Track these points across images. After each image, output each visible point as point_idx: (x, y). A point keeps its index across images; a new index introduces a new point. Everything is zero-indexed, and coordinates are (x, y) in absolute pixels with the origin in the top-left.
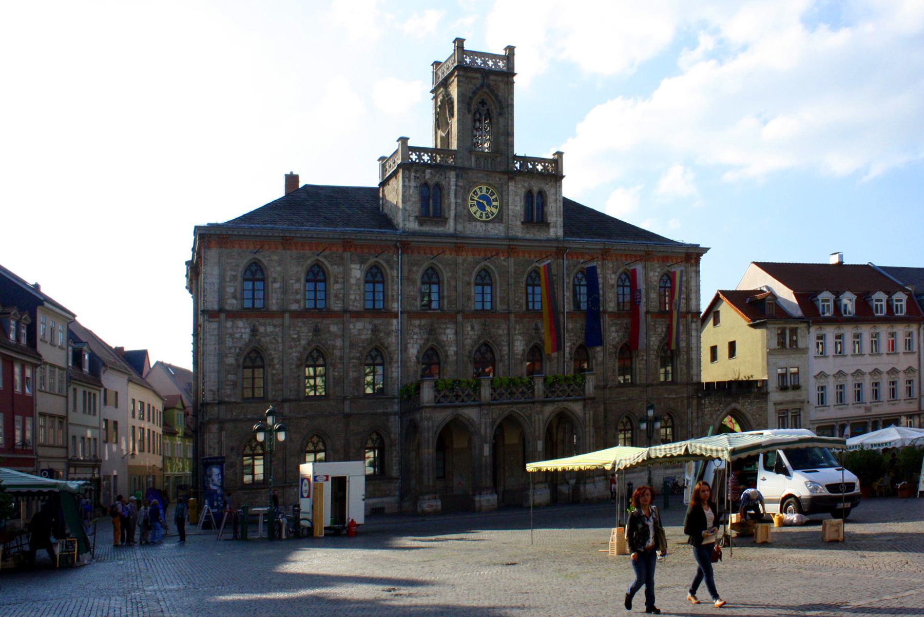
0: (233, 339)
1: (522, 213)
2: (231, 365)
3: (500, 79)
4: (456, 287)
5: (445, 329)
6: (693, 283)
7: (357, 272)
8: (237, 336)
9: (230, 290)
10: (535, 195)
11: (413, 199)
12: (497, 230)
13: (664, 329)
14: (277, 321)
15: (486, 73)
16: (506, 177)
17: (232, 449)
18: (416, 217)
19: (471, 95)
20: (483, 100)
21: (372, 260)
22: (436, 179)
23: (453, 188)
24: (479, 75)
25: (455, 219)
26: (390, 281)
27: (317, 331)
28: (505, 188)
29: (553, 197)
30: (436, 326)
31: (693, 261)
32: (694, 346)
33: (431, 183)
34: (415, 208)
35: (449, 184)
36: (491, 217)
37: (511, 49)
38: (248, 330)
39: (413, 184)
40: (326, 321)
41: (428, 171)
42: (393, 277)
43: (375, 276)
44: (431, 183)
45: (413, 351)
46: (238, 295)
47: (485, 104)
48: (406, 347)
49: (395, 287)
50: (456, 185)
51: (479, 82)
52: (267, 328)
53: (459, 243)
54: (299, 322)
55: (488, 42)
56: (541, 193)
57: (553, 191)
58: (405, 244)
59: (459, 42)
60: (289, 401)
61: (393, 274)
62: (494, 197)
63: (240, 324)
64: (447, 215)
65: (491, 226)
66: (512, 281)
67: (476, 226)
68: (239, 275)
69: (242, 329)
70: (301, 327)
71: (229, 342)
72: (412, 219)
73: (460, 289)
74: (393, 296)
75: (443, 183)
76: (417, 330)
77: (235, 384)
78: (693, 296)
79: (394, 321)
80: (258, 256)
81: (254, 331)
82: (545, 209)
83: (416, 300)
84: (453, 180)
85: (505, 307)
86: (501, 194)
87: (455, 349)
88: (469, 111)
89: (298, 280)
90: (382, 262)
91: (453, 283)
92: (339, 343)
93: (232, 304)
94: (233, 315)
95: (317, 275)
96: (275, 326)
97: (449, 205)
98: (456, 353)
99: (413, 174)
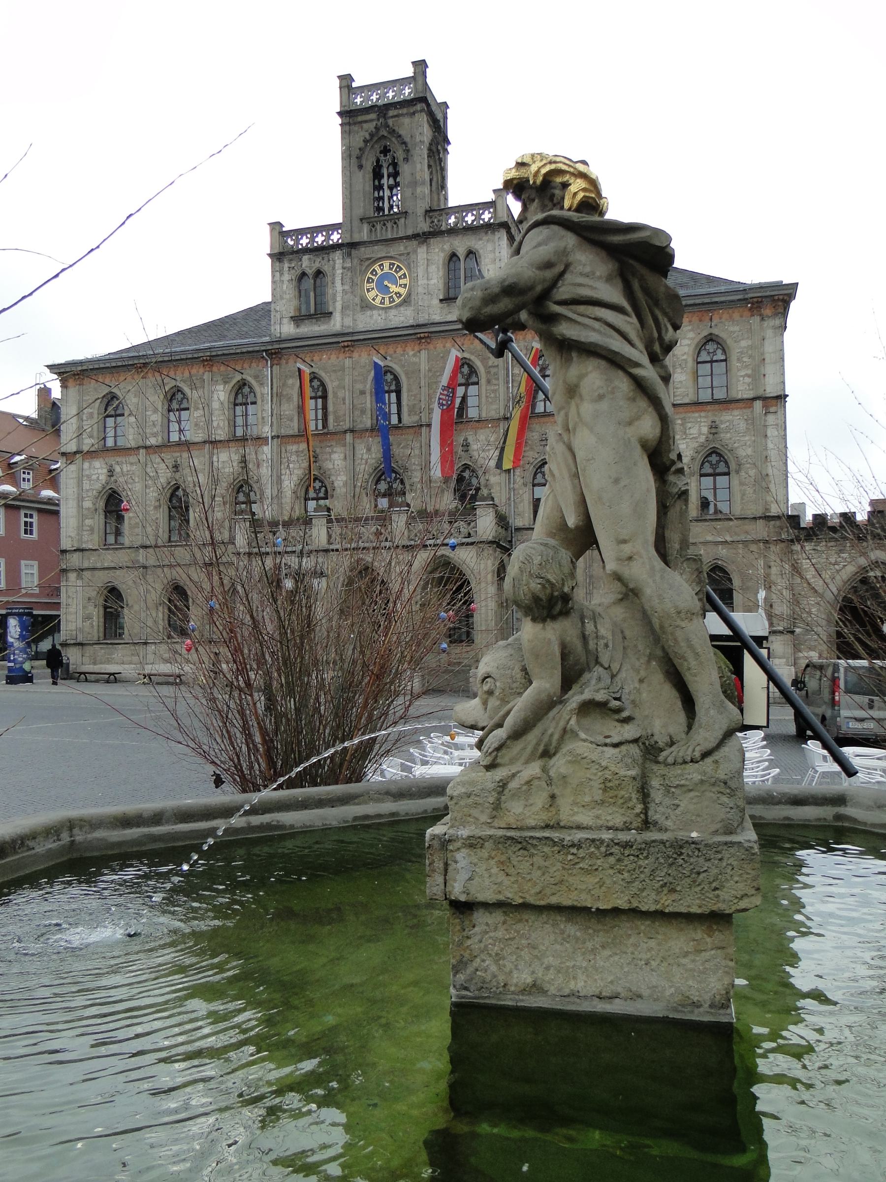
0: (90, 481)
1: (441, 286)
2: (88, 509)
3: (405, 111)
4: (344, 399)
5: (330, 454)
6: (769, 348)
7: (221, 394)
8: (94, 477)
10: (462, 258)
11: (288, 296)
12: (403, 317)
13: (705, 430)
14: (133, 459)
15: (382, 110)
16: (415, 243)
18: (292, 317)
19: (362, 144)
20: (385, 147)
21: (238, 377)
22: (317, 265)
23: (339, 272)
24: (373, 116)
25: (342, 311)
26: (259, 402)
28: (413, 256)
29: (491, 256)
30: (318, 450)
31: (768, 311)
32: (773, 454)
33: (310, 272)
34: (288, 306)
35: (334, 268)
36: (397, 301)
37: (421, 66)
38: (105, 471)
39: (286, 277)
41: (306, 258)
42: (263, 395)
43: (242, 394)
44: (310, 272)
45: (289, 483)
46: (95, 434)
47: (390, 151)
48: (280, 481)
49: (266, 407)
50: (344, 268)
51: (371, 126)
53: (347, 342)
54: (156, 459)
55: (381, 67)
56: (470, 253)
57: (490, 247)
58: (275, 352)
59: (346, 81)
60: (146, 547)
61: (264, 391)
62: (400, 274)
63: (97, 463)
64: (331, 310)
65: (393, 312)
66: (422, 384)
67: (371, 316)
68: (96, 412)
69: (98, 470)
70: (159, 463)
71: (86, 486)
72: (285, 321)
73: (347, 402)
74: (263, 418)
75: (326, 268)
76: (294, 458)
77: (92, 530)
78: (769, 369)
81: (111, 472)
83: (291, 420)
84: (339, 262)
85: (416, 418)
86: (409, 268)
87: (344, 478)
88: (360, 167)
89: (156, 410)
90: (249, 379)
91: (340, 394)
94: (91, 454)
95: (175, 400)
96: (132, 464)
97: (335, 295)
98: (345, 484)
99: (286, 265)
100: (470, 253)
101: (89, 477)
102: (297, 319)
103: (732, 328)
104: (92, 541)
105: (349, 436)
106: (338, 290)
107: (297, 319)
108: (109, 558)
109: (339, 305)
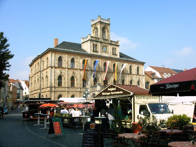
7: (81, 61)
9: (56, 62)
17: (56, 97)
22: (96, 44)
27: (74, 73)
39: (92, 44)
40: (75, 71)
46: (57, 64)
52: (63, 71)
54: (70, 71)
63: (58, 70)
79: (89, 72)
80: (62, 56)
81: (61, 72)
82: (116, 52)
89: (69, 62)
92: (78, 76)
93: (57, 66)
95: (73, 60)
100: (115, 48)
101: (56, 72)
102: (94, 51)
103: (140, 66)
104: (57, 86)
105: (101, 72)
106: (99, 48)
107: (94, 51)
108: (60, 89)
109: (99, 51)
